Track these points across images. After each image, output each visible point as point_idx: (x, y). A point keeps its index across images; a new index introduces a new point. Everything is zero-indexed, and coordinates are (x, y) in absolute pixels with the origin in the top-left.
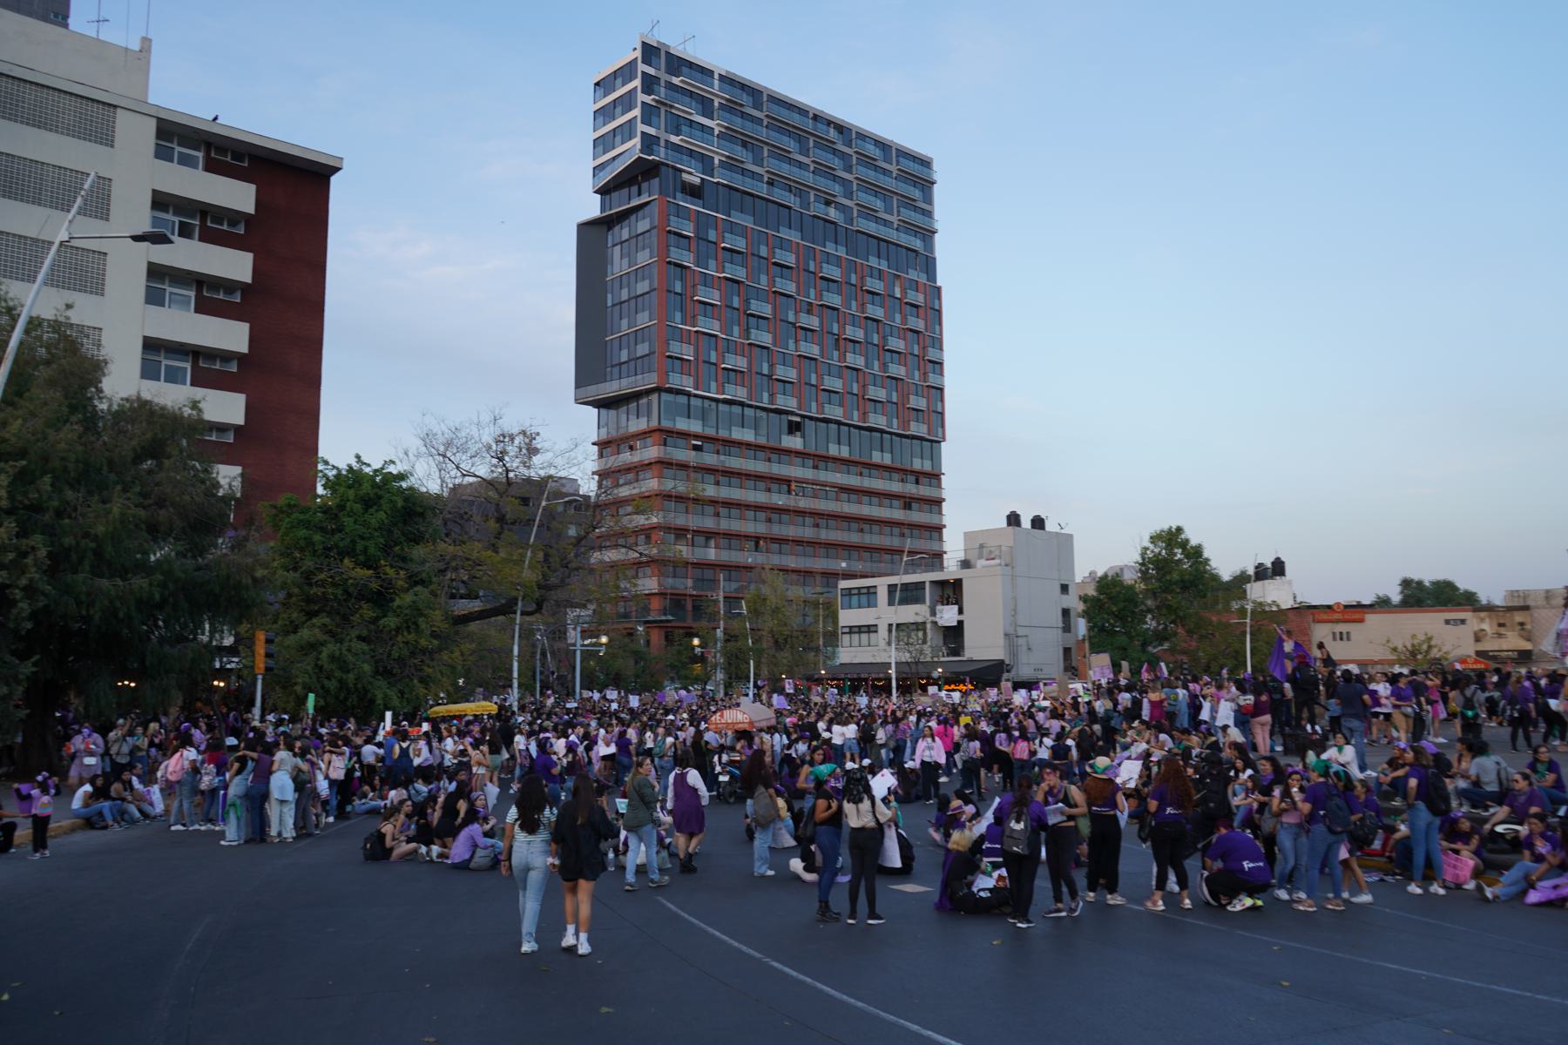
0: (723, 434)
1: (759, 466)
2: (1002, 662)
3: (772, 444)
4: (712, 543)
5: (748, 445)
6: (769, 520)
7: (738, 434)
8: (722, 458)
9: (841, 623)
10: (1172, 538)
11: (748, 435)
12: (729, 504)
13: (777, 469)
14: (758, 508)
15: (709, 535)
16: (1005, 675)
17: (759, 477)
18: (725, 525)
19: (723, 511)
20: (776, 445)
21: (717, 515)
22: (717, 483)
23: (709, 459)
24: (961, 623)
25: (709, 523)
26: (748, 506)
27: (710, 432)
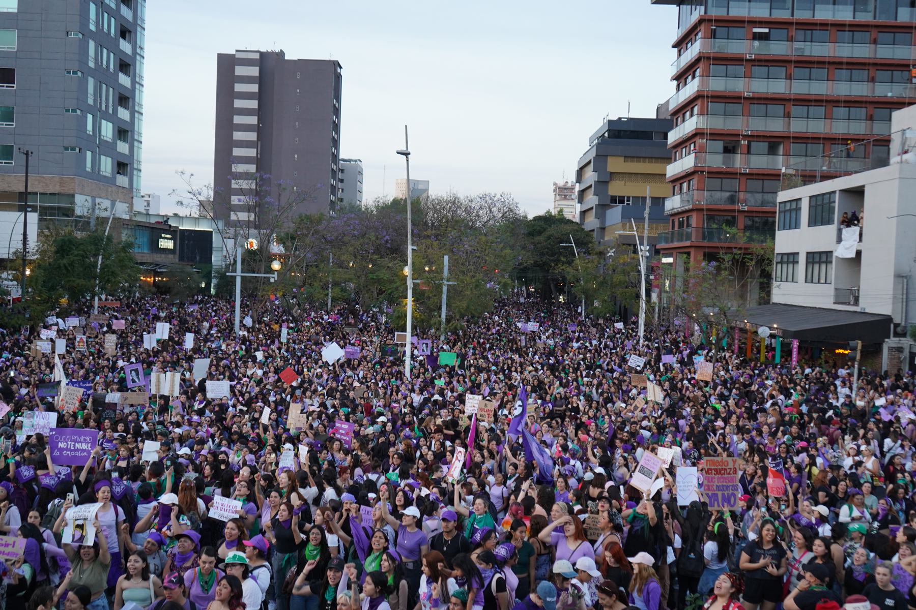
0: (802, 15)
1: (861, 51)
2: (888, 320)
3: (882, 20)
4: (781, 150)
5: (840, 26)
6: (870, 118)
7: (824, 13)
8: (798, 45)
9: (777, 251)
10: (337, 64)
11: (845, 14)
12: (804, 101)
13: (886, 52)
14: (850, 103)
15: (773, 143)
16: (891, 342)
17: (853, 65)
18: (798, 126)
19: (795, 110)
20: (892, 22)
21: (788, 115)
22: (789, 77)
23: (778, 48)
24: (859, 253)
25: (776, 126)
26: (835, 102)
27: (782, 14)
